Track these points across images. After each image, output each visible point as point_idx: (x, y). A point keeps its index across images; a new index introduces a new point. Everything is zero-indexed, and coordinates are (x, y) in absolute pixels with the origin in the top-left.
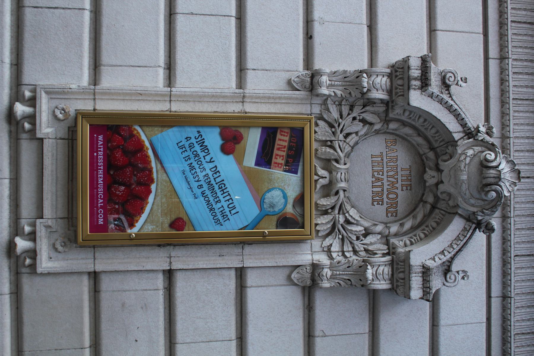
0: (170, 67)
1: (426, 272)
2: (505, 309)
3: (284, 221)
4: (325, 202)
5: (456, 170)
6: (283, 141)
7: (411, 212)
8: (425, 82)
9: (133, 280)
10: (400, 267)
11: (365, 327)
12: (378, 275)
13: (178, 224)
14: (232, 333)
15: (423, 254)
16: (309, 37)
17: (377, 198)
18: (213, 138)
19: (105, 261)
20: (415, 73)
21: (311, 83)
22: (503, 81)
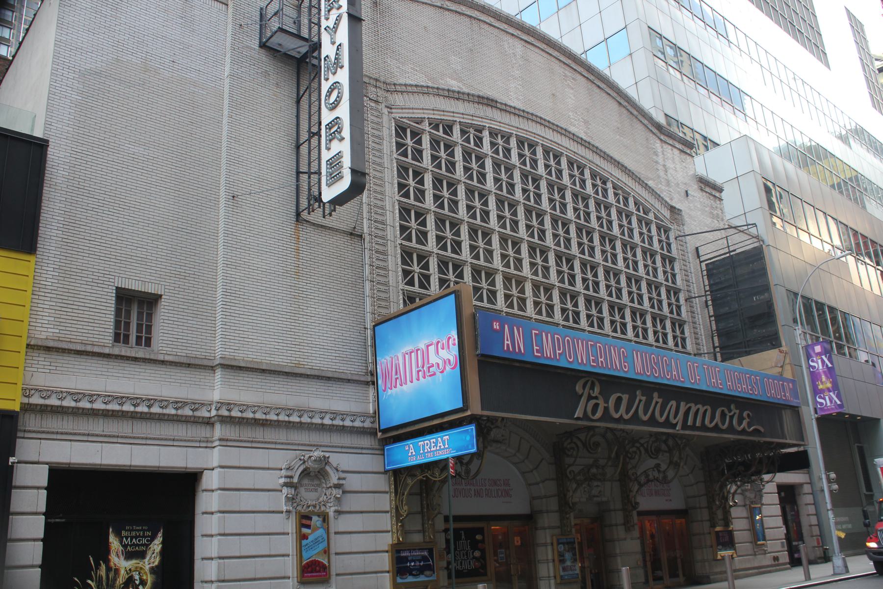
0: (283, 556)
1: (339, 479)
2: (345, 447)
3: (324, 521)
4: (318, 508)
5: (314, 468)
6: (304, 521)
7: (319, 479)
8: (291, 477)
9: (337, 564)
10: (338, 486)
11: (348, 495)
12: (337, 493)
13: (325, 552)
14: (349, 536)
15: (334, 479)
16: (273, 512)
17: (316, 490)
18: (304, 542)
19: (333, 572)
20: (288, 480)
21: (288, 512)
22: (282, 444)
